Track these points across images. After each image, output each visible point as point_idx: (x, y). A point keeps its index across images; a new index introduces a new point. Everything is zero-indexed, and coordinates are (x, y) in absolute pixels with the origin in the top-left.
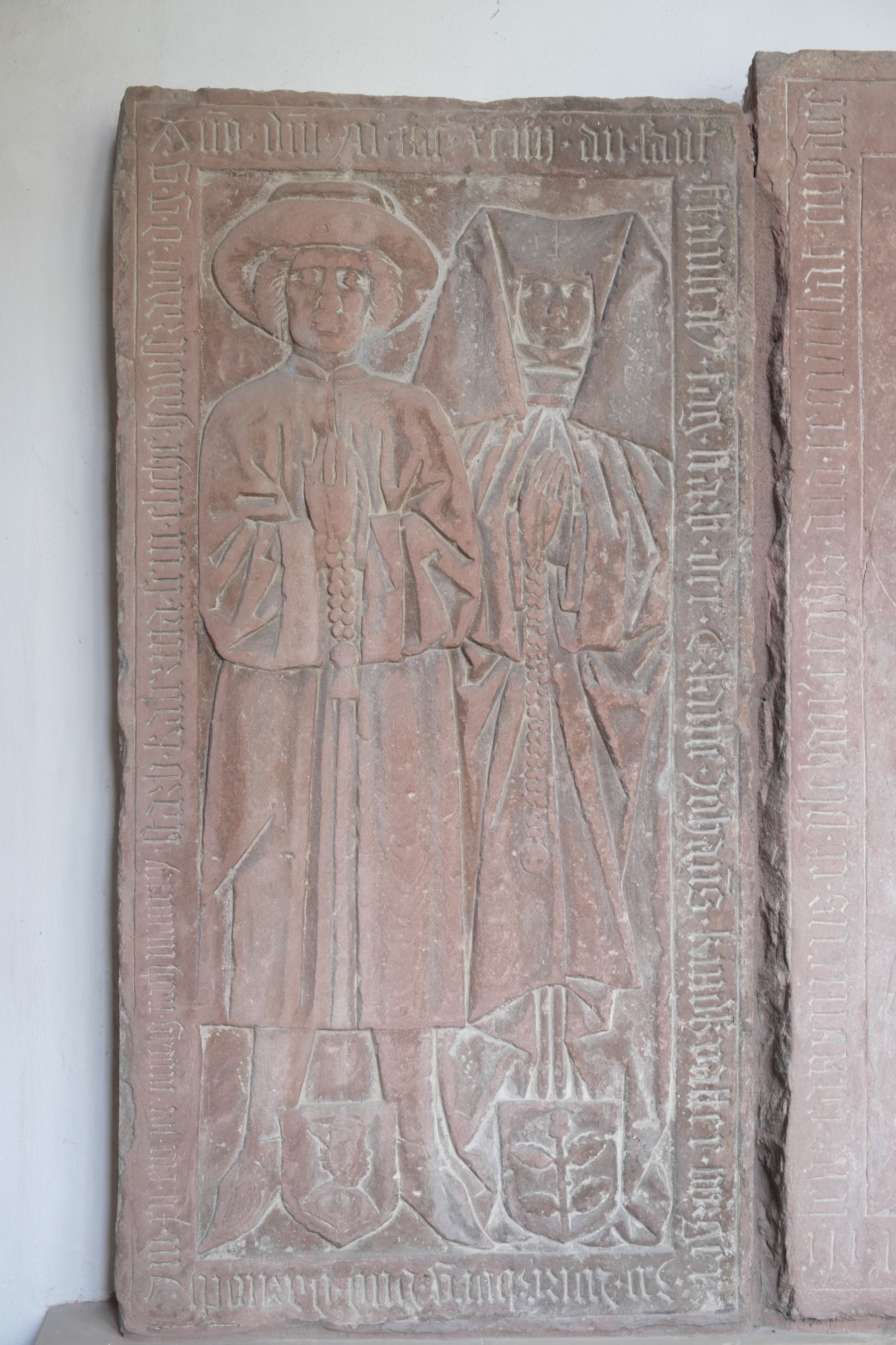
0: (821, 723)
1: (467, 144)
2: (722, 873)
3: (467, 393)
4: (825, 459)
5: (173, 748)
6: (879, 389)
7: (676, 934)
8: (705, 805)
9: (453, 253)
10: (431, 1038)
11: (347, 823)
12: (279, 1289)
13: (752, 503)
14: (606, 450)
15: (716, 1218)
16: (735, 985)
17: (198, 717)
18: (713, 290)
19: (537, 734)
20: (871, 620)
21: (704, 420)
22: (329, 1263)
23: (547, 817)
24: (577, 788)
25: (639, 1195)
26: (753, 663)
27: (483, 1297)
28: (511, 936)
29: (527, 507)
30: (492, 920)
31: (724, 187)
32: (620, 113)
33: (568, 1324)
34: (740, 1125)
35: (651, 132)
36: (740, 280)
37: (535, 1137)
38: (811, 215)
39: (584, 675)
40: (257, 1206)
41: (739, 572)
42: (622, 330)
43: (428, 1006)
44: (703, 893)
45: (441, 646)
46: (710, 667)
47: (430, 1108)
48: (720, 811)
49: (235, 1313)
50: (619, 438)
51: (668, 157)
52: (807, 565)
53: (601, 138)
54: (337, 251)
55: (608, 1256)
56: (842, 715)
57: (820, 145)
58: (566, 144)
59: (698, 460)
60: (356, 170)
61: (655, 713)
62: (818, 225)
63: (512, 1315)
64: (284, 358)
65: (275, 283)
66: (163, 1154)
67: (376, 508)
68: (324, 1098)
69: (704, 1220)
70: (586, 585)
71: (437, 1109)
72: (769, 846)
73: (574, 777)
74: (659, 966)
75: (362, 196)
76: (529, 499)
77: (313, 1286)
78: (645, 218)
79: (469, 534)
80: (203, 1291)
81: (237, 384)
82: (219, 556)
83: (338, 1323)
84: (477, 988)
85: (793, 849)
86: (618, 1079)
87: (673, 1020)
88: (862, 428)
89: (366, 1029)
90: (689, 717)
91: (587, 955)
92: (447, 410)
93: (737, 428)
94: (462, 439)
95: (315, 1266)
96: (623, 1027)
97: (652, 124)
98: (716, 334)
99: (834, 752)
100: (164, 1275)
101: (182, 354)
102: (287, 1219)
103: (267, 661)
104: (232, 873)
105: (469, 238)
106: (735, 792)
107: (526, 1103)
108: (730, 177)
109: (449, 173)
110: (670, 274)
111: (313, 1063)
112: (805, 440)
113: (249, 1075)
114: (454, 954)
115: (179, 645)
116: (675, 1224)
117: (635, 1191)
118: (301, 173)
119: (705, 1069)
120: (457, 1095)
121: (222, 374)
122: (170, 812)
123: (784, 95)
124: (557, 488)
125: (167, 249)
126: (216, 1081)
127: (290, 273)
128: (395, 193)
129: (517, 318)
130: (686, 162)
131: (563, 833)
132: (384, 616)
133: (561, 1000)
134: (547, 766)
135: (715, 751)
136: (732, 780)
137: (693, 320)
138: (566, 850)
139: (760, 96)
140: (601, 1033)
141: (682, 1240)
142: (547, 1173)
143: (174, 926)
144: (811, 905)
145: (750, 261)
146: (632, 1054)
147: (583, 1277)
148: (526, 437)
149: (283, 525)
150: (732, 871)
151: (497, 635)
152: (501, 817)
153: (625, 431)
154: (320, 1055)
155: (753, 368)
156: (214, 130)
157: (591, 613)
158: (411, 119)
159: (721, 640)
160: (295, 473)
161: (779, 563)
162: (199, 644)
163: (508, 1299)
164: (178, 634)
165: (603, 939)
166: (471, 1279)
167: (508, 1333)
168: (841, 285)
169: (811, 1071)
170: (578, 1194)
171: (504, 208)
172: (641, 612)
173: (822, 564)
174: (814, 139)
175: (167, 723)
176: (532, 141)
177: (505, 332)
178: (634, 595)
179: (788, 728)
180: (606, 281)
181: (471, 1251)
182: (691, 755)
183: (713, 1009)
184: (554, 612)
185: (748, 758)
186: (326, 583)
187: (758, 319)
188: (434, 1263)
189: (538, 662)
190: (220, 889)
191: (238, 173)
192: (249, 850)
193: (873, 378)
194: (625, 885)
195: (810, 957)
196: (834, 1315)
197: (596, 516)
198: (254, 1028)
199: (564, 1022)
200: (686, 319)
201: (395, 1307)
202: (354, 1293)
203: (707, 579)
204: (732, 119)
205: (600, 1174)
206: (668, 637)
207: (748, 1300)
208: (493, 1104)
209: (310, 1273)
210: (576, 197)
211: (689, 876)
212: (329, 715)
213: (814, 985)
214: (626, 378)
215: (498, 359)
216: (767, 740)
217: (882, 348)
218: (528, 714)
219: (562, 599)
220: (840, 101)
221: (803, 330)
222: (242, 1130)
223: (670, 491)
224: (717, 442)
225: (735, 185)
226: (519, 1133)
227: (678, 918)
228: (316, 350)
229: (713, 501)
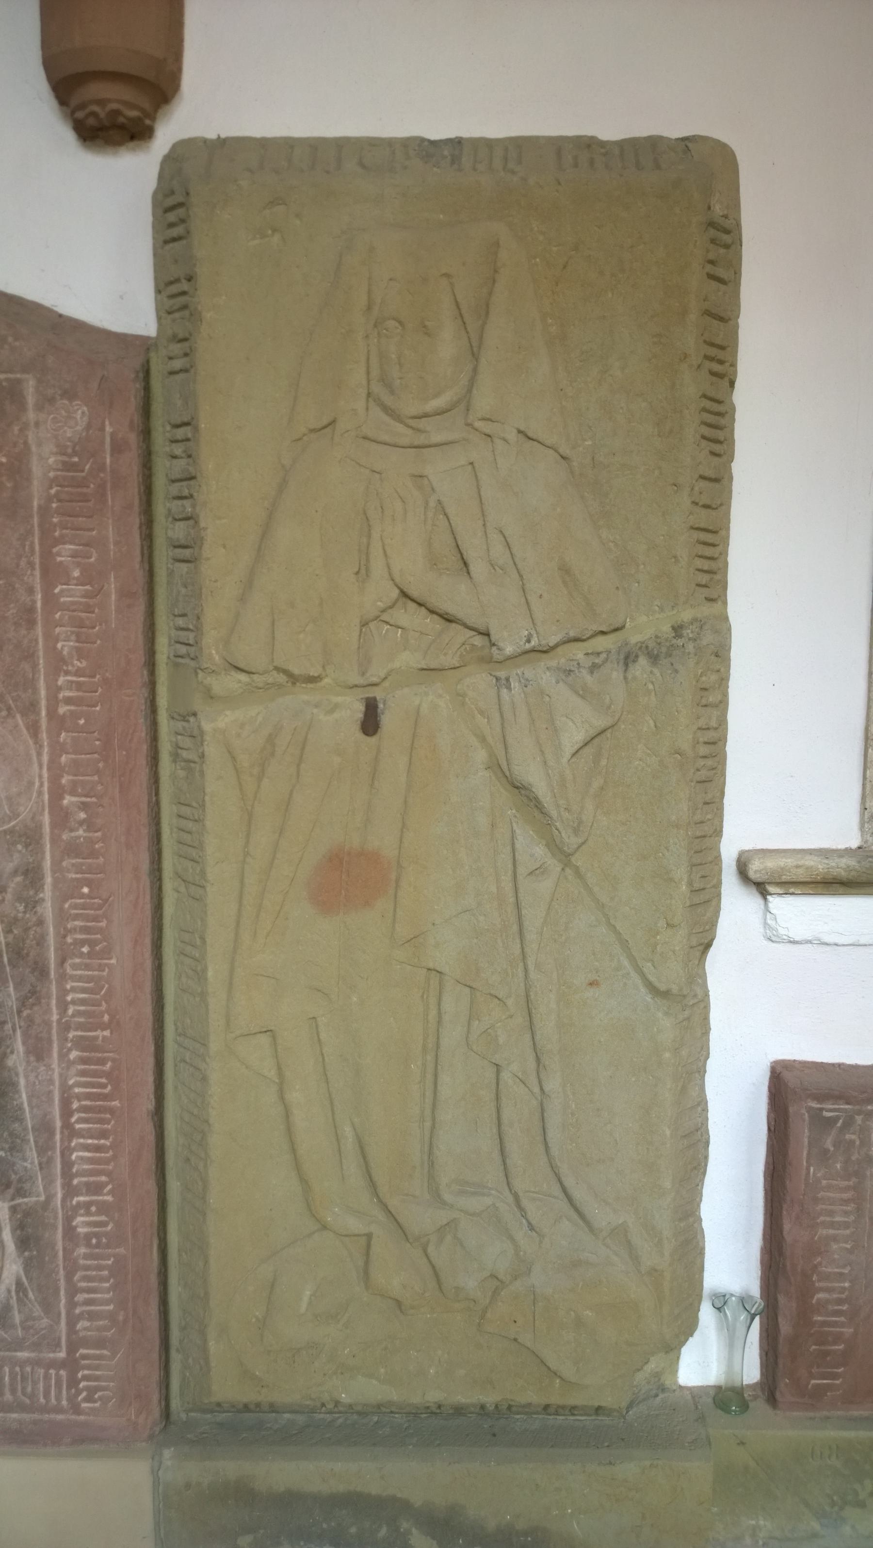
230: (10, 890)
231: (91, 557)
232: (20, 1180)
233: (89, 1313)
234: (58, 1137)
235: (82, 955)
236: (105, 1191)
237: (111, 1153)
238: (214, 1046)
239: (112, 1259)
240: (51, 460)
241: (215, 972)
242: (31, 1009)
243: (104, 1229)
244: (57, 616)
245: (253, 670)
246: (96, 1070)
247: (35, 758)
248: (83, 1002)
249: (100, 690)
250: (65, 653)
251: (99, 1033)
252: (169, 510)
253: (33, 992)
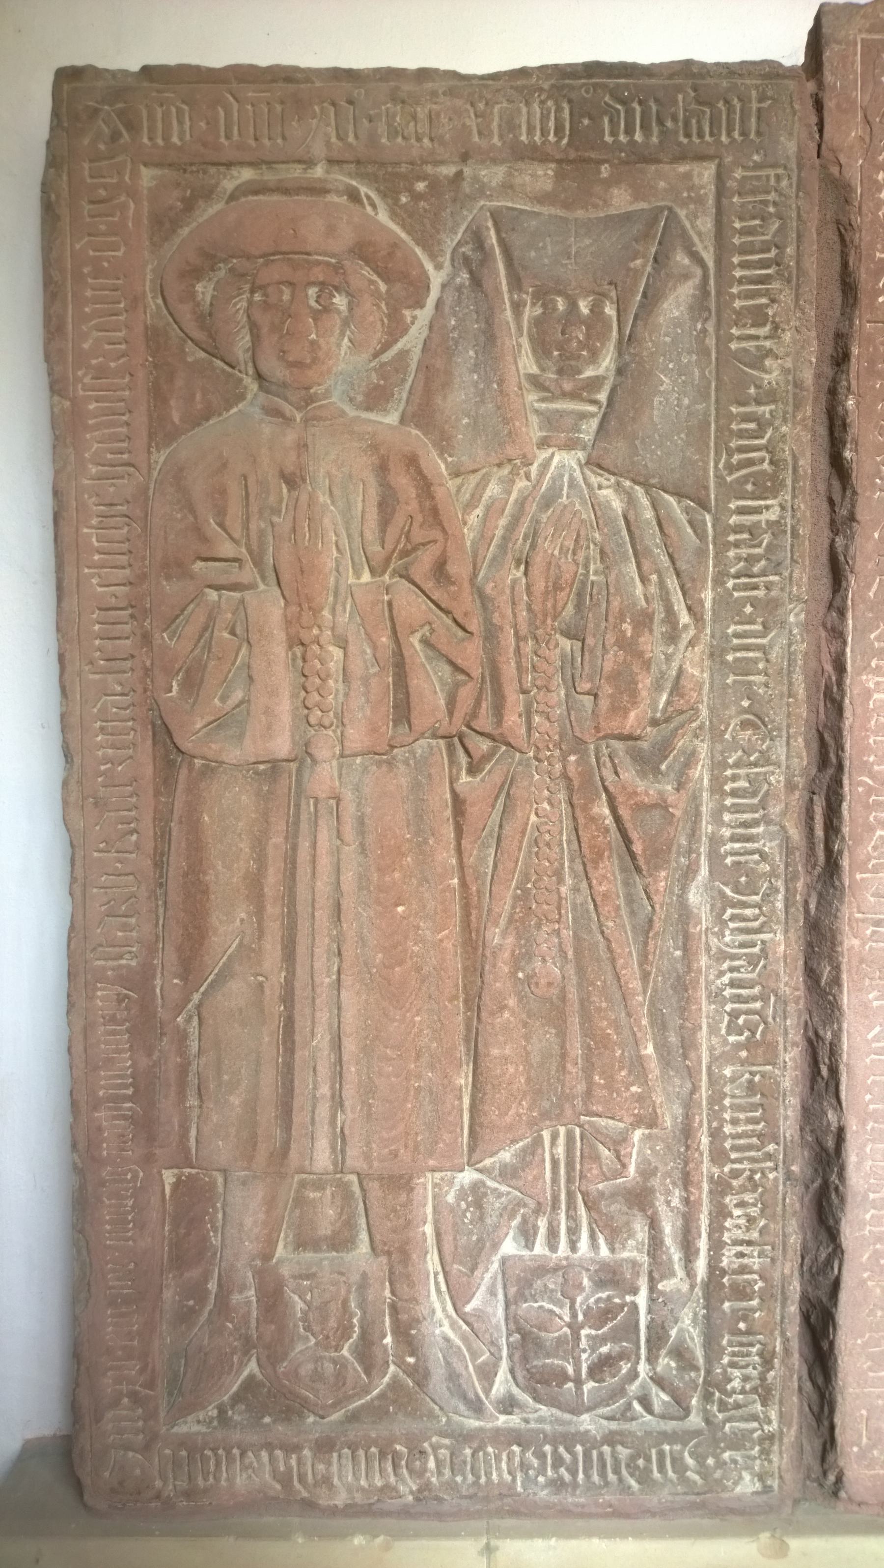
1: (464, 125)
3: (464, 435)
5: (125, 855)
7: (709, 1068)
8: (745, 919)
9: (447, 263)
10: (427, 1182)
11: (327, 940)
12: (255, 1464)
13: (807, 563)
14: (631, 501)
15: (754, 1390)
16: (779, 1127)
17: (155, 819)
18: (764, 301)
19: (547, 837)
21: (750, 463)
22: (311, 1437)
23: (558, 933)
24: (594, 900)
25: (666, 1363)
26: (805, 754)
27: (486, 1475)
28: (517, 1070)
29: (537, 570)
30: (495, 1052)
31: (780, 171)
32: (653, 81)
33: (583, 1506)
34: (783, 1287)
35: (690, 104)
36: (798, 286)
37: (546, 1297)
39: (603, 769)
40: (229, 1374)
41: (790, 645)
42: (652, 353)
43: (422, 1148)
44: (741, 1021)
45: (435, 736)
46: (752, 758)
47: (425, 1262)
49: (206, 1491)
50: (646, 486)
51: (712, 134)
52: (872, 636)
53: (630, 113)
54: (307, 261)
55: (630, 1432)
58: (586, 122)
59: (741, 511)
60: (331, 162)
61: (685, 812)
63: (519, 1495)
64: (249, 397)
65: (235, 304)
66: (122, 1315)
67: (358, 575)
68: (304, 1250)
69: (740, 1393)
70: (606, 663)
71: (433, 1262)
72: (819, 964)
73: (590, 887)
74: (689, 1105)
75: (338, 193)
76: (538, 560)
77: (293, 1462)
78: (682, 213)
79: (468, 603)
80: (170, 1466)
81: (194, 428)
82: (175, 632)
83: (322, 1502)
84: (478, 1129)
85: (849, 971)
86: (641, 1231)
87: (706, 1166)
89: (351, 1173)
90: (727, 817)
91: (605, 1092)
92: (441, 455)
93: (790, 472)
94: (458, 490)
95: (295, 1440)
96: (647, 1172)
97: (693, 94)
98: (767, 356)
100: (128, 1447)
101: (127, 393)
102: (264, 1386)
103: (233, 754)
104: (196, 997)
105: (467, 243)
106: (780, 905)
107: (534, 1258)
108: (788, 157)
109: (442, 162)
110: (712, 282)
111: (292, 1211)
112: (874, 484)
113: (219, 1224)
114: (452, 1091)
115: (131, 737)
116: (707, 1397)
117: (660, 1360)
118: (264, 167)
119: (742, 1221)
120: (456, 1247)
121: (176, 417)
122: (125, 928)
123: (856, 54)
124: (572, 547)
125: (106, 264)
126: (182, 1231)
127: (252, 292)
128: (378, 190)
129: (525, 341)
130: (733, 141)
131: (578, 952)
132: (368, 701)
133: (574, 1142)
134: (559, 875)
135: (756, 857)
136: (777, 891)
137: (740, 338)
138: (581, 970)
139: (827, 54)
140: (621, 1180)
141: (715, 1416)
142: (559, 1339)
143: (130, 1058)
144: (870, 1036)
145: (811, 264)
146: (657, 1204)
147: (601, 1455)
148: (534, 487)
149: (248, 595)
150: (776, 995)
151: (499, 722)
152: (504, 934)
153: (654, 477)
154: (300, 1201)
155: (811, 397)
156: (159, 116)
157: (611, 696)
158: (394, 98)
159: (766, 726)
160: (262, 533)
161: (837, 634)
162: (154, 735)
163: (514, 1479)
164: (130, 724)
165: (623, 1073)
166: (473, 1455)
167: (515, 1513)
169: (868, 1228)
170: (593, 1364)
171: (510, 205)
172: (671, 694)
175: (120, 826)
176: (544, 118)
177: (510, 358)
178: (663, 674)
179: (846, 830)
180: (633, 293)
181: (474, 1423)
182: (729, 860)
183: (752, 1154)
184: (567, 695)
185: (796, 865)
186: (300, 662)
187: (818, 337)
188: (430, 1438)
189: (549, 753)
190: (184, 1015)
191: (189, 169)
192: (216, 971)
194: (649, 1010)
197: (617, 581)
198: (224, 1171)
199: (578, 1167)
200: (731, 338)
201: (387, 1487)
202: (340, 1470)
204: (792, 85)
205: (621, 1340)
206: (703, 723)
207: (788, 1477)
208: (496, 1259)
209: (291, 1449)
210: (598, 189)
211: (725, 1001)
212: (304, 817)
213: (873, 1129)
214: (656, 412)
215: (501, 391)
216: (816, 840)
218: (537, 814)
219: (577, 680)
221: (876, 349)
222: (212, 1286)
223: (708, 549)
224: (766, 489)
225: (794, 166)
226: (527, 1292)
227: (711, 1049)
228: (284, 385)
229: (759, 561)
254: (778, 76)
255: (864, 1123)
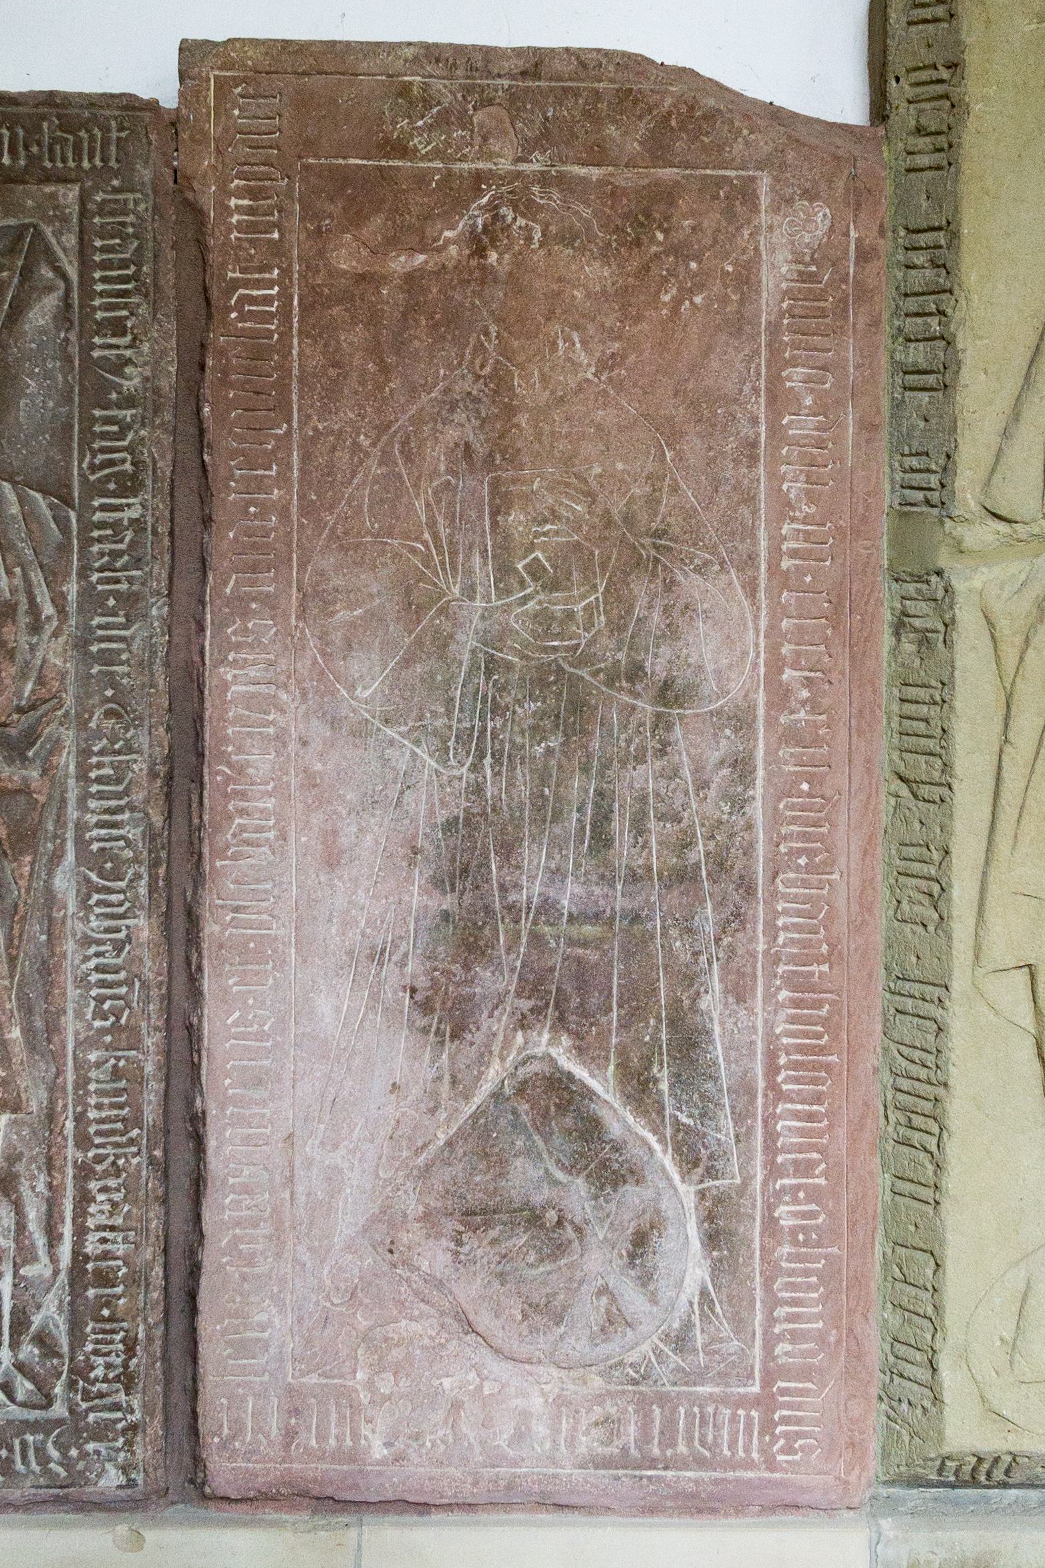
0: (242, 812)
2: (129, 983)
4: (252, 509)
6: (315, 429)
7: (74, 1052)
15: (117, 1379)
16: (142, 1112)
18: (125, 313)
20: (304, 695)
21: (111, 463)
25: (28, 1351)
31: (139, 195)
38: (239, 227)
44: (106, 1006)
46: (116, 747)
48: (126, 912)
50: (14, 484)
52: (229, 631)
56: (270, 804)
57: (250, 147)
59: (104, 508)
62: (246, 239)
69: (103, 1382)
74: (54, 1089)
78: (48, 231)
85: (209, 957)
87: (71, 1151)
88: (296, 473)
90: (93, 804)
97: (57, 122)
99: (258, 846)
106: (143, 890)
110: (75, 295)
112: (228, 487)
116: (71, 1385)
117: (24, 1347)
119: (107, 1207)
123: (208, 89)
130: (94, 167)
135: (122, 843)
141: (77, 1405)
144: (229, 1022)
145: (168, 280)
146: (22, 1189)
168: (274, 309)
169: (228, 1212)
173: (247, 628)
174: (244, 140)
178: (27, 663)
182: (95, 846)
183: (117, 1139)
193: (309, 417)
195: (228, 1081)
196: (252, 1494)
200: (93, 347)
203: (114, 646)
211: (89, 986)
213: (232, 1114)
214: (22, 413)
217: (319, 382)
220: (275, 97)
224: (126, 488)
225: (150, 192)
227: (77, 1033)
229: (121, 557)
230: (713, 786)
231: (824, 383)
232: (711, 1157)
233: (792, 1332)
234: (760, 1101)
235: (798, 869)
236: (817, 1172)
237: (826, 1122)
238: (960, 983)
239: (823, 1262)
240: (784, 270)
241: (963, 891)
242: (732, 936)
243: (813, 1222)
244: (784, 452)
245: (1019, 519)
246: (811, 1016)
247: (750, 624)
248: (797, 928)
249: (831, 540)
250: (792, 496)
251: (814, 968)
252: (900, 330)
253: (737, 915)
254: (134, 108)
255: (223, 1110)
